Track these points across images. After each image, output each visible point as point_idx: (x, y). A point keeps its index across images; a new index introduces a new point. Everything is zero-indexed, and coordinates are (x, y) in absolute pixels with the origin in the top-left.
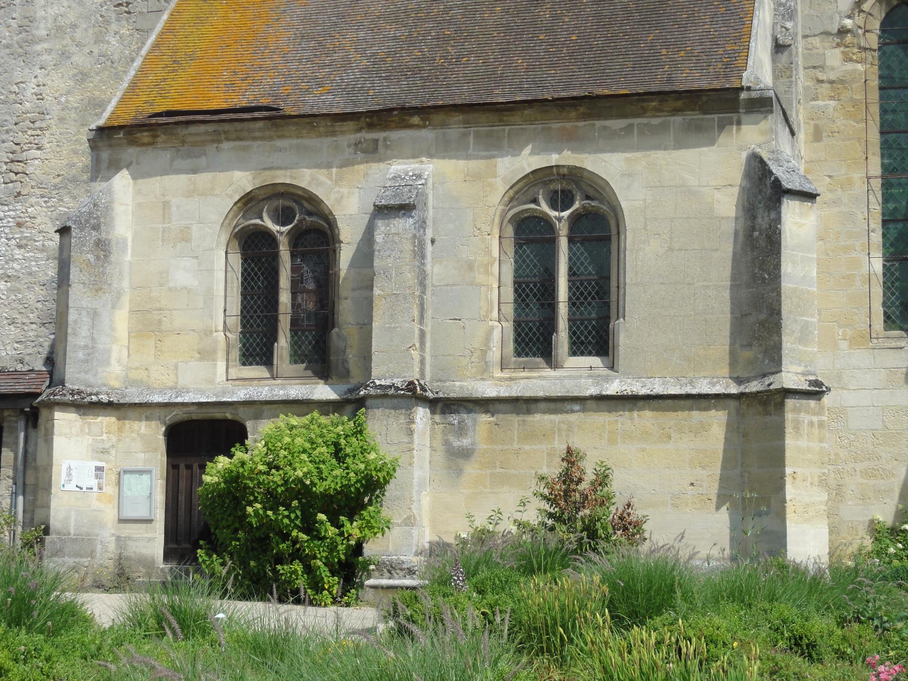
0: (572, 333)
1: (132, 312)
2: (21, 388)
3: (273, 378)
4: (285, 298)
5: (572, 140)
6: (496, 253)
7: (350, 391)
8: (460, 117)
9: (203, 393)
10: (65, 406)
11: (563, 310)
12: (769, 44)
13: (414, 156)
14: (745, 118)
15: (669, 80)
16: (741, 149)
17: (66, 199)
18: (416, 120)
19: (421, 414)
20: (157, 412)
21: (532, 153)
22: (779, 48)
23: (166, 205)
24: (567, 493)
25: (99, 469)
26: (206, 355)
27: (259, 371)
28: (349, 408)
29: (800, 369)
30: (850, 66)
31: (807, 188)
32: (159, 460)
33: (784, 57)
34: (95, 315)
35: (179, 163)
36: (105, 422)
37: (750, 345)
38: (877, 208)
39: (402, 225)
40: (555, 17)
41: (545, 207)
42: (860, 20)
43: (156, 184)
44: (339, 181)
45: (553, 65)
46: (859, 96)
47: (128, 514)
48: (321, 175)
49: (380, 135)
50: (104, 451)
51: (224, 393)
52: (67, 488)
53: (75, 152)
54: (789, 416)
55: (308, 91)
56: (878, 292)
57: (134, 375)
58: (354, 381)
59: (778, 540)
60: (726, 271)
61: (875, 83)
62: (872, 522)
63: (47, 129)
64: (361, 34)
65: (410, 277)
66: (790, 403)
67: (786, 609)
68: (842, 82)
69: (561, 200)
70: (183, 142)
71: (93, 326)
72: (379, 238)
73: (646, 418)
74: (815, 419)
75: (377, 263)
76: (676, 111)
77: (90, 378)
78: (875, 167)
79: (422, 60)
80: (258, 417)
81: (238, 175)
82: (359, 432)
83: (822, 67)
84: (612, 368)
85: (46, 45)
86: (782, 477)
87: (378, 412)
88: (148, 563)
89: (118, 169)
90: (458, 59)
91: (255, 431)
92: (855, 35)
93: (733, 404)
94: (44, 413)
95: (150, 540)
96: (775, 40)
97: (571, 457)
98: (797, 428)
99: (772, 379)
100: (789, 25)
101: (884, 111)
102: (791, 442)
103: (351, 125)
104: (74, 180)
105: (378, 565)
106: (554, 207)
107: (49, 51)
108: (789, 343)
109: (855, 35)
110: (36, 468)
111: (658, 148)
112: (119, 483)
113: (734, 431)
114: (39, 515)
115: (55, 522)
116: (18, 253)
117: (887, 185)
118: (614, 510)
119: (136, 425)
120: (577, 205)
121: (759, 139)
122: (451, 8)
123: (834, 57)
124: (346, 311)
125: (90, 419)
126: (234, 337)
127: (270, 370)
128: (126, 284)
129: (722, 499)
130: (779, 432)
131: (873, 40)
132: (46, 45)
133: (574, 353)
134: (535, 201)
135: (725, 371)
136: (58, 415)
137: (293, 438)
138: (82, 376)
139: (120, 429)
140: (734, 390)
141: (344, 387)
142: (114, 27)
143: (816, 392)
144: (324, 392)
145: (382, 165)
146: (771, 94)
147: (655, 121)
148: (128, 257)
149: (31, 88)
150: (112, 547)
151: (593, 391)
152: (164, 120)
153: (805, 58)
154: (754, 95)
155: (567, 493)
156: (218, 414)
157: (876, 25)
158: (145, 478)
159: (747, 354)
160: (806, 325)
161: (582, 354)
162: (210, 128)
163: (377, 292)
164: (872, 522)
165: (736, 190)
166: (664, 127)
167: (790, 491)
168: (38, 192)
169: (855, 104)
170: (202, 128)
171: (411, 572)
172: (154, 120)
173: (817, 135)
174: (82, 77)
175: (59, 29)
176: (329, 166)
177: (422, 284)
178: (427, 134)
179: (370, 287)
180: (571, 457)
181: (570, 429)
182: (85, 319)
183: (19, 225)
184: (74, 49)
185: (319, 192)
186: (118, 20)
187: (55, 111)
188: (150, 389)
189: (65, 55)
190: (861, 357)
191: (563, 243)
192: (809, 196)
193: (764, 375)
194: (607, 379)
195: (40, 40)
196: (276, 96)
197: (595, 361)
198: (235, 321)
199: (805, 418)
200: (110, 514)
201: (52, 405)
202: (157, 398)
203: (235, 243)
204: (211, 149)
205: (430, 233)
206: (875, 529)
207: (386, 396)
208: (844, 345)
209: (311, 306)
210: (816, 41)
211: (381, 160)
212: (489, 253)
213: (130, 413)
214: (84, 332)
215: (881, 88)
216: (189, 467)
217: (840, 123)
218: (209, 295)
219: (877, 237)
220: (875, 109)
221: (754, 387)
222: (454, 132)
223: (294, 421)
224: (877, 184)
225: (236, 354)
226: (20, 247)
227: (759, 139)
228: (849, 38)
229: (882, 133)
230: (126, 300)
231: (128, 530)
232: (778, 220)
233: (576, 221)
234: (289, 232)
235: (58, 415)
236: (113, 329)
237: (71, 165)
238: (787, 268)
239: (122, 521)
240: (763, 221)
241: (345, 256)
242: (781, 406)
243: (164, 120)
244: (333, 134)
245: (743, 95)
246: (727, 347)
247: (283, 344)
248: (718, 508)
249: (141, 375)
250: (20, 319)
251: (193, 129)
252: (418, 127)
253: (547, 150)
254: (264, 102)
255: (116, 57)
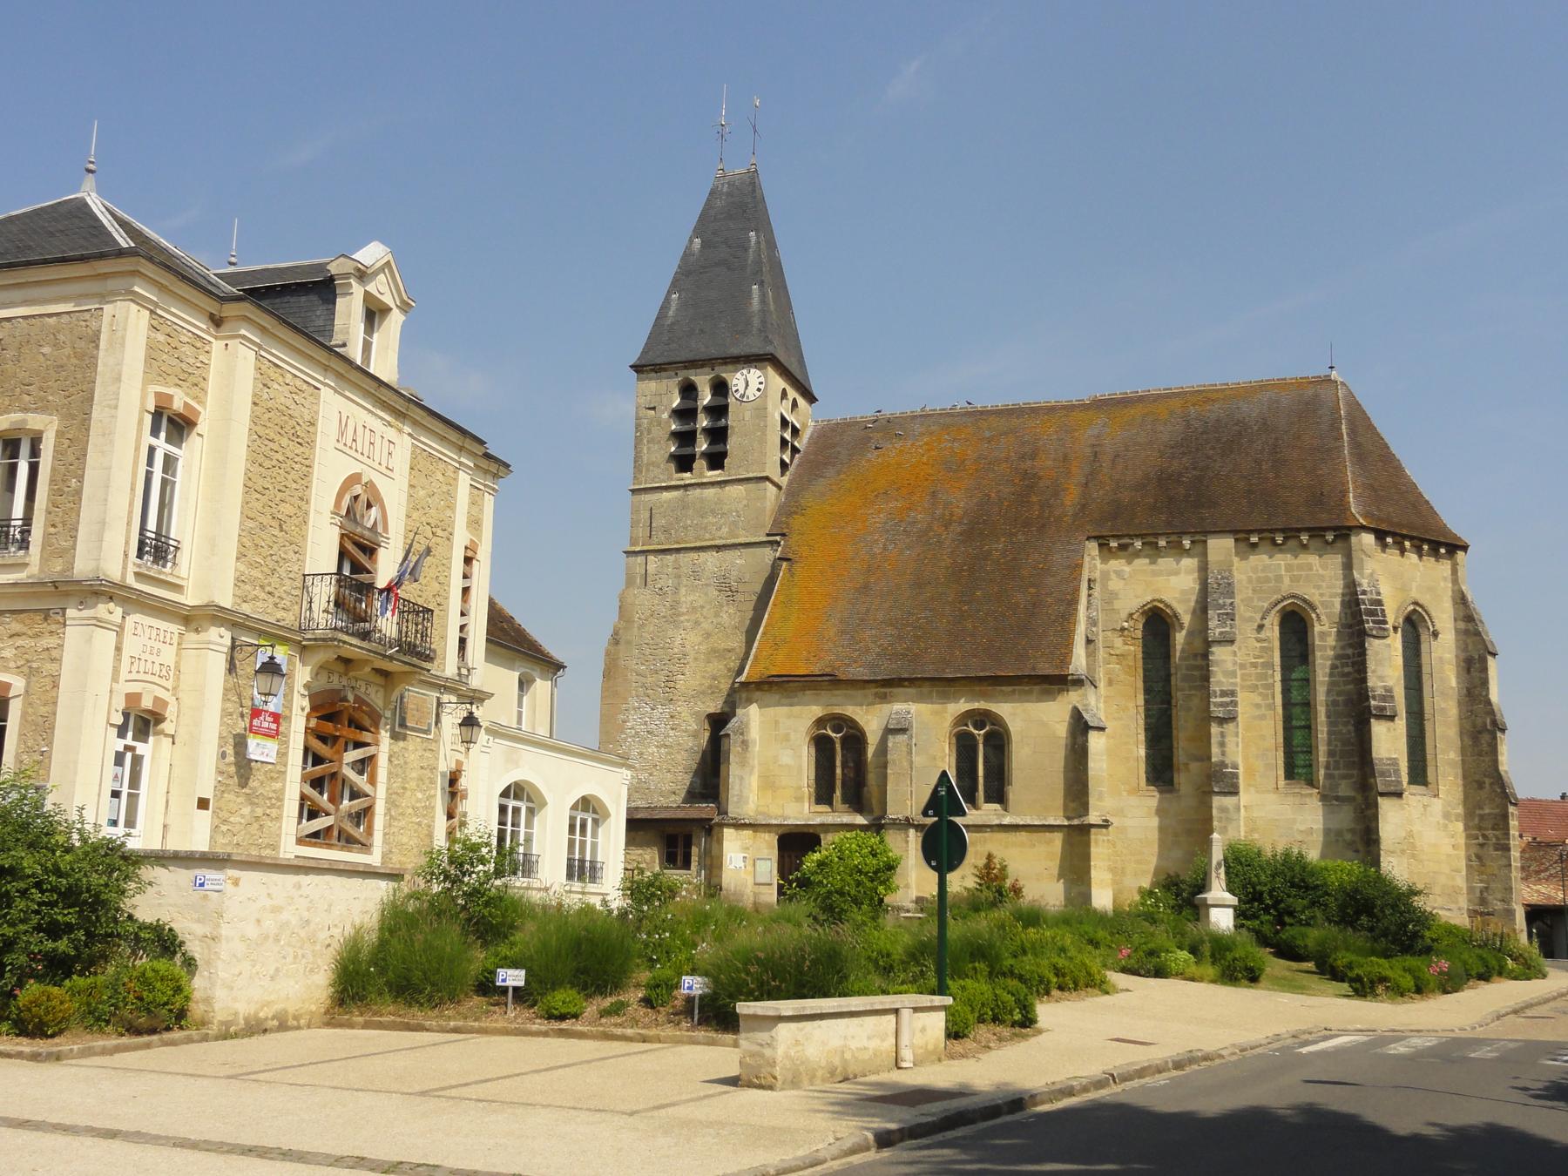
0: (986, 792)
1: (759, 777)
2: (704, 816)
3: (833, 811)
4: (839, 771)
5: (985, 696)
6: (947, 751)
7: (874, 820)
8: (927, 683)
9: (797, 819)
10: (729, 825)
11: (981, 780)
12: (1083, 641)
13: (906, 701)
14: (1070, 688)
15: (1034, 669)
16: (1069, 703)
17: (699, 703)
18: (906, 683)
19: (912, 832)
20: (774, 829)
21: (966, 702)
22: (1089, 641)
23: (777, 722)
24: (988, 873)
25: (745, 857)
26: (799, 799)
27: (825, 808)
28: (874, 829)
29: (1098, 814)
30: (1127, 647)
31: (1101, 725)
32: (774, 854)
33: (1092, 646)
34: (741, 778)
35: (783, 701)
36: (748, 833)
37: (1074, 801)
38: (1142, 722)
39: (901, 738)
40: (974, 627)
41: (971, 729)
42: (1132, 623)
43: (772, 711)
44: (867, 711)
45: (975, 656)
46: (1131, 663)
47: (760, 880)
48: (858, 709)
49: (887, 690)
50: (748, 849)
51: (809, 820)
52: (732, 867)
53: (704, 677)
54: (1093, 837)
55: (849, 665)
56: (1142, 767)
57: (761, 809)
58: (877, 813)
59: (1087, 897)
60: (1062, 764)
61: (1140, 655)
62: (1140, 888)
63: (688, 663)
64: (874, 632)
65: (905, 764)
66: (1093, 830)
67: (1088, 928)
68: (1122, 655)
69: (979, 725)
70: (786, 690)
71: (741, 785)
72: (890, 745)
73: (1023, 836)
74: (1105, 838)
75: (889, 757)
76: (1036, 684)
77: (739, 811)
78: (1141, 700)
79: (907, 649)
80: (827, 832)
81: (814, 707)
82: (882, 841)
83: (1112, 647)
84: (1006, 810)
85: (686, 617)
86: (1090, 866)
87: (891, 832)
88: (769, 906)
89: (751, 703)
90: (927, 649)
91: (825, 839)
92: (1129, 631)
93: (1066, 829)
94: (716, 830)
95: (771, 894)
96: (1087, 637)
97: (990, 857)
98: (1096, 843)
99: (1084, 818)
100: (1094, 629)
101: (1145, 670)
102: (1092, 849)
103: (873, 685)
104: (703, 693)
105: (893, 908)
106: (976, 728)
107: (688, 621)
108: (1092, 801)
109: (1129, 631)
110: (711, 857)
111: (1028, 701)
112: (754, 865)
113: (1068, 845)
114: (715, 880)
115: (724, 885)
116: (671, 733)
117: (1147, 710)
118: (1008, 883)
119: (763, 835)
120: (987, 728)
121: (1079, 699)
122: (920, 619)
123: (1118, 642)
124: (872, 778)
125: (740, 832)
126: (812, 790)
127: (832, 808)
128: (756, 762)
129: (1060, 876)
130: (1088, 845)
131: (1139, 634)
132: (686, 617)
133: (986, 802)
134: (967, 725)
135: (1062, 814)
136: (725, 830)
137: (850, 844)
138: (737, 810)
139: (755, 837)
140: (1066, 823)
141: (871, 818)
142: (725, 608)
143: (1106, 825)
144: (860, 820)
145: (889, 705)
146: (1084, 677)
147: (1027, 688)
148: (757, 749)
149: (678, 641)
150: (752, 899)
151: (996, 822)
152: (776, 679)
153: (1103, 641)
154: (1075, 677)
155: (988, 873)
156: (806, 830)
157: (1141, 626)
158: (769, 862)
159: (1072, 805)
160: (1101, 792)
161: (990, 802)
162: (801, 684)
163: (889, 771)
164: (1140, 888)
165: (1066, 724)
166: (1030, 692)
167: (1094, 873)
168: (683, 699)
169: (1129, 667)
170: (797, 684)
171: (908, 911)
172: (771, 679)
173: (1110, 683)
174: (708, 635)
175: (694, 608)
176: (861, 705)
177: (911, 768)
178: (912, 691)
179: (886, 767)
180: (990, 857)
181: (985, 841)
182: (737, 781)
183: (672, 717)
184: (702, 620)
185: (857, 718)
186: (727, 605)
187: (692, 654)
188: (771, 817)
189: (697, 623)
190: (1134, 801)
191: (981, 747)
192: (1102, 729)
193: (1081, 816)
194: (1003, 816)
195: (683, 614)
196: (834, 668)
197: (997, 806)
198: (812, 782)
199: (1100, 838)
200: (750, 881)
201: (722, 825)
202: (775, 822)
203: (812, 742)
204: (800, 694)
205: (914, 740)
206: (1141, 891)
207: (895, 824)
208: (1125, 794)
209: (852, 775)
210: (1109, 633)
211: (889, 702)
212: (944, 751)
213: (761, 829)
214: (737, 787)
215: (1143, 658)
216: (790, 857)
217: (1122, 677)
218: (800, 767)
219: (1142, 737)
220: (1141, 671)
221: (1076, 822)
222: (925, 690)
223: (848, 835)
224: (1142, 710)
225: (813, 799)
226: (673, 729)
227: (1079, 699)
228: (1126, 633)
229: (1144, 682)
230: (756, 770)
231: (757, 889)
232: (1087, 741)
233: (987, 737)
234: (841, 737)
235: (725, 830)
236: (750, 784)
237: (701, 685)
238: (1091, 764)
239: (755, 884)
240: (1080, 740)
241: (871, 751)
242: (1088, 833)
243: (776, 679)
244: (864, 689)
245: (1070, 678)
246: (1062, 801)
247: (838, 793)
248: (1058, 881)
249: (765, 809)
250: (673, 769)
251: (791, 684)
252: (910, 687)
253: (972, 701)
254: (828, 670)
255: (726, 625)
